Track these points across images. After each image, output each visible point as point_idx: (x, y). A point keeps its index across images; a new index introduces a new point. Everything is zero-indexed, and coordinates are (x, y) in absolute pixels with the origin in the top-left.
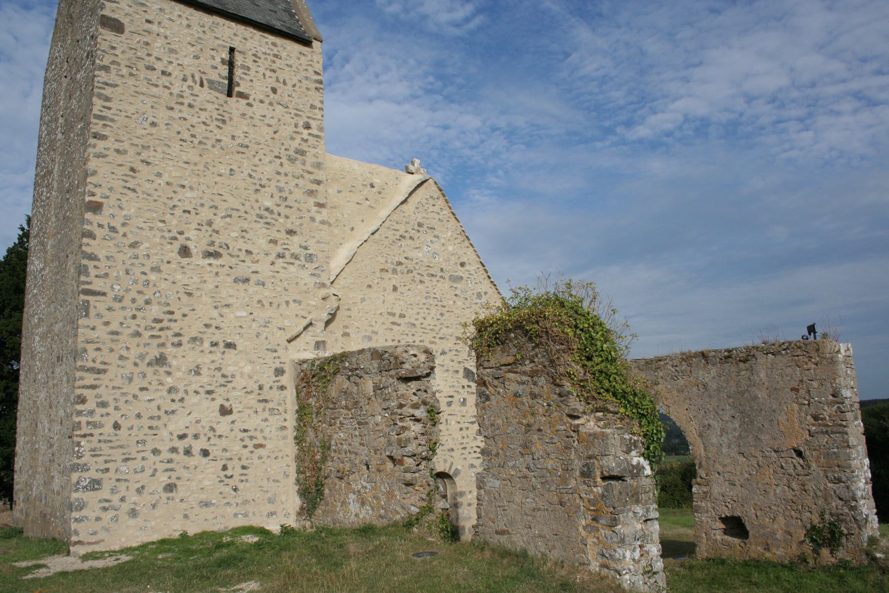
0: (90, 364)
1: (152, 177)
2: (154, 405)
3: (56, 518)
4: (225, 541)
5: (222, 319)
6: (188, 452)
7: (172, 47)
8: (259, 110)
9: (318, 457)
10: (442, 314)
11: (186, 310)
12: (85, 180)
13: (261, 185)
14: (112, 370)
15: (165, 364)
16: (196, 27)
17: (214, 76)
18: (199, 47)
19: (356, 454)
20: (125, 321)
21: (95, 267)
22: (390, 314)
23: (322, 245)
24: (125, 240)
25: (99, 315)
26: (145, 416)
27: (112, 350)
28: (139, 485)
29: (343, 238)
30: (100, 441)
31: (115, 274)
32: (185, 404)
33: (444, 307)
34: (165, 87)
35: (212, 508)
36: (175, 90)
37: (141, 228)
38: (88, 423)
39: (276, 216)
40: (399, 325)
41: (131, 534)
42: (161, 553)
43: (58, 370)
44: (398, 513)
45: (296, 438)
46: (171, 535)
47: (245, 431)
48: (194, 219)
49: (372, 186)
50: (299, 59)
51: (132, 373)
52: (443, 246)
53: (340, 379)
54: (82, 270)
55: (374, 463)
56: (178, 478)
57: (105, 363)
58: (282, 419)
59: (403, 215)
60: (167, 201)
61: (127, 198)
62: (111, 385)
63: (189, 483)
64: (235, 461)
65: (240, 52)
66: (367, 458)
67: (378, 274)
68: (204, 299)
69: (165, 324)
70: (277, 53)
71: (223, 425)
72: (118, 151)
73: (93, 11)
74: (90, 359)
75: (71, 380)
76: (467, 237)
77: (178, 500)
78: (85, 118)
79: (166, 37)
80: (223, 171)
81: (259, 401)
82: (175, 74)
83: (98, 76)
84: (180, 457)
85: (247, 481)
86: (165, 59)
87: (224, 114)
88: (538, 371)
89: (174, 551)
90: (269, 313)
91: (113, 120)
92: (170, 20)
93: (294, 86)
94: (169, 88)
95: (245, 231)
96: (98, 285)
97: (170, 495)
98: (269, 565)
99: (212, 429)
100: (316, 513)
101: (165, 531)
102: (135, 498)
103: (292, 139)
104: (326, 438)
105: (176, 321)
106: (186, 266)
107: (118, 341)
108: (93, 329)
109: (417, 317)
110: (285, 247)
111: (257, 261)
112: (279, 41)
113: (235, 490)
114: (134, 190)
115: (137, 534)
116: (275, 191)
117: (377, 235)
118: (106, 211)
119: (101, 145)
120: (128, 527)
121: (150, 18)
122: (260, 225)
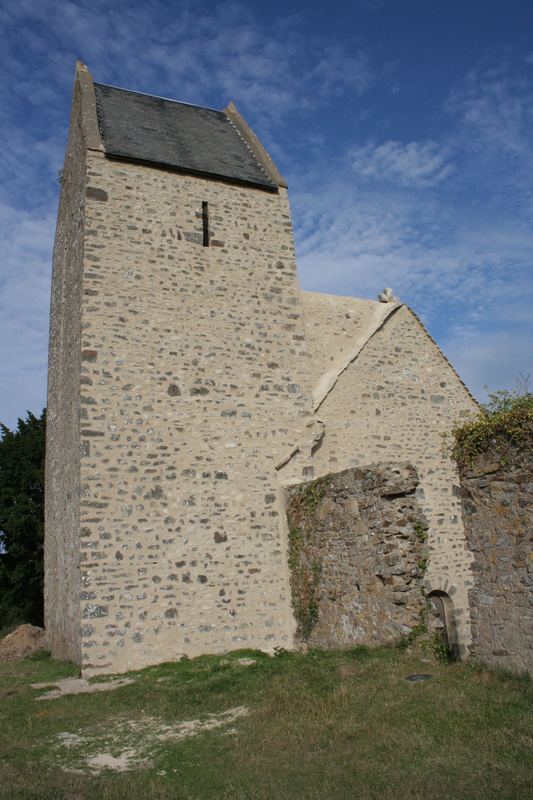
0: (92, 499)
1: (140, 325)
2: (153, 535)
3: (72, 642)
4: (221, 664)
5: (212, 451)
6: (186, 579)
7: (151, 207)
8: (233, 255)
9: (311, 579)
10: (426, 435)
11: (178, 445)
12: (81, 332)
13: (241, 324)
14: (113, 504)
15: (161, 496)
16: (170, 188)
17: (190, 229)
18: (175, 204)
19: (347, 575)
20: (122, 458)
21: (93, 410)
22: (375, 437)
23: (304, 375)
24: (118, 384)
25: (98, 454)
26: (145, 545)
27: (111, 486)
28: (142, 611)
29: (324, 368)
30: (104, 570)
31: (111, 415)
32: (182, 533)
33: (428, 427)
34: (147, 243)
35: (212, 632)
36: (156, 245)
37: (133, 372)
38: (93, 554)
39: (257, 351)
40: (384, 447)
41: (137, 658)
42: (161, 676)
43: (68, 506)
44: (390, 634)
45: (289, 562)
46: (173, 658)
47: (240, 556)
48: (181, 360)
49: (348, 317)
50: (267, 205)
51: (131, 506)
52: (422, 367)
53: (327, 501)
54: (83, 414)
55: (364, 583)
56: (178, 604)
57: (106, 498)
58: (275, 544)
59: (380, 341)
60: (155, 345)
61: (118, 345)
62: (112, 518)
63: (188, 608)
64: (232, 586)
65: (212, 205)
66: (357, 579)
67: (360, 400)
68: (194, 433)
69: (159, 458)
70: (246, 202)
71: (219, 552)
72: (108, 304)
73: (82, 186)
74: (92, 494)
75: (78, 515)
76: (445, 358)
77: (179, 625)
78: (78, 280)
79: (145, 200)
80: (204, 314)
81: (253, 527)
82: (154, 231)
83: (87, 240)
84: (179, 584)
85: (244, 605)
86: (145, 219)
87: (202, 262)
88: (526, 476)
89: (173, 675)
90: (256, 443)
91: (102, 277)
92: (148, 184)
93: (265, 230)
94: (150, 244)
95: (229, 367)
96: (96, 426)
97: (171, 620)
98: (261, 689)
99: (209, 556)
100: (312, 634)
101: (169, 654)
102: (139, 624)
103: (267, 278)
104: (317, 560)
105: (169, 455)
106: (176, 404)
107: (116, 476)
108: (94, 466)
109: (402, 438)
110: (268, 379)
111: (243, 395)
112: (247, 191)
113: (233, 614)
114: (124, 338)
115: (142, 657)
116: (255, 329)
117: (356, 363)
118: (100, 359)
119: (92, 300)
120: (133, 651)
121: (129, 185)
122: (242, 361)
